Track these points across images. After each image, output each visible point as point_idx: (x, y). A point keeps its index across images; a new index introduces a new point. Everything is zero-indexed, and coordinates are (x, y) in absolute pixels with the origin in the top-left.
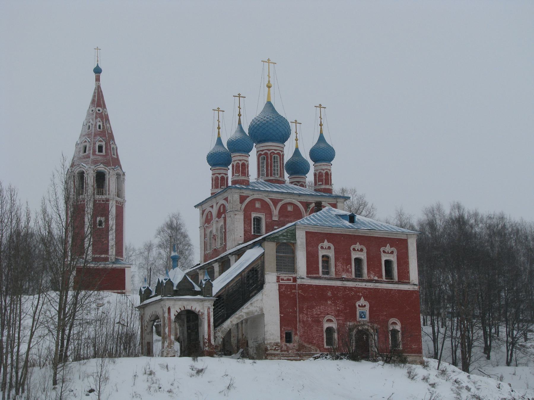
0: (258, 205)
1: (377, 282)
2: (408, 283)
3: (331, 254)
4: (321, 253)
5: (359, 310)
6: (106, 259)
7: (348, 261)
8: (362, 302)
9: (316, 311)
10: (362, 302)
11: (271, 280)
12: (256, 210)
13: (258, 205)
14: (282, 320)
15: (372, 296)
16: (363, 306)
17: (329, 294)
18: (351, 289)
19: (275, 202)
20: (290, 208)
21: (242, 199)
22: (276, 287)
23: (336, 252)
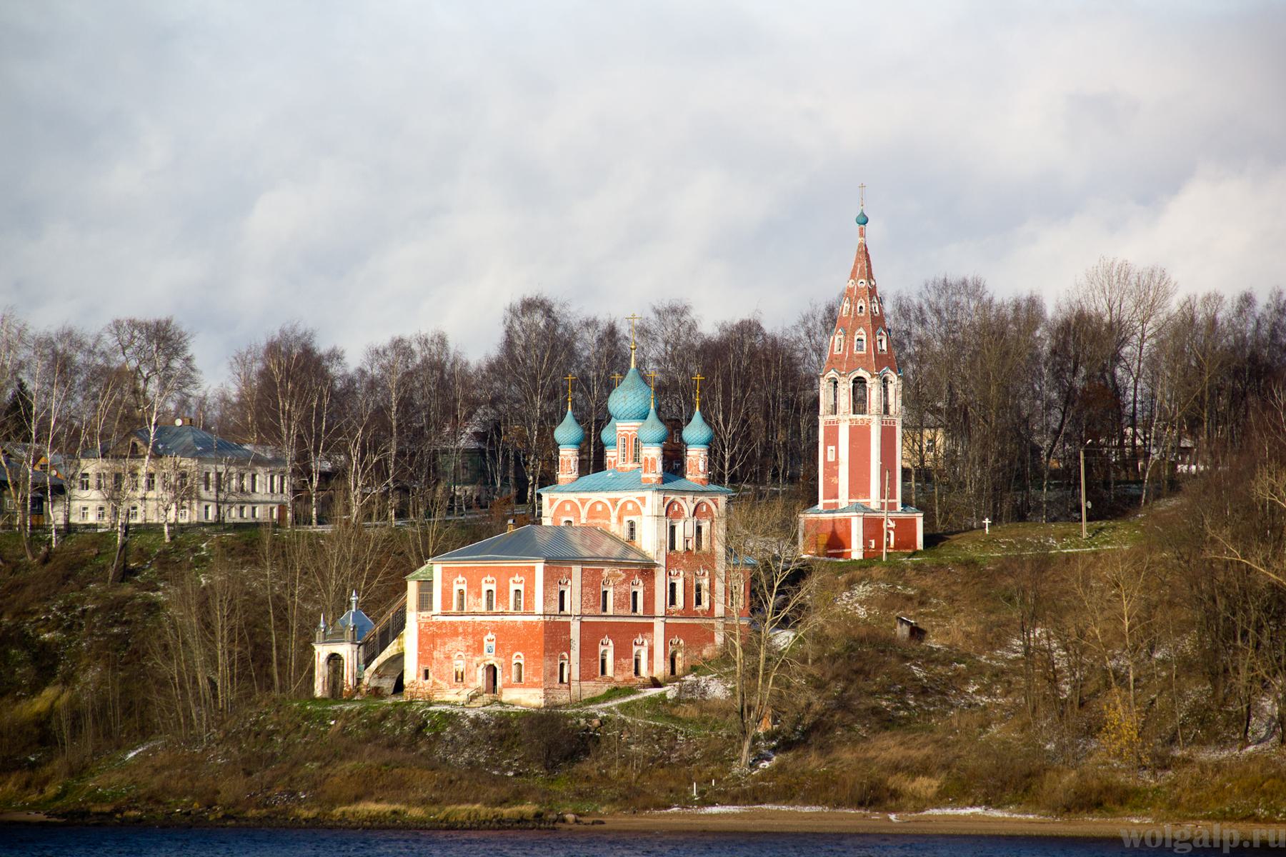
0: (568, 507)
1: (503, 614)
2: (533, 614)
3: (464, 587)
4: (456, 588)
5: (486, 644)
6: (836, 505)
7: (479, 595)
8: (490, 636)
9: (449, 647)
10: (490, 636)
11: (412, 618)
12: (567, 514)
13: (568, 507)
14: (419, 657)
15: (500, 630)
16: (489, 640)
17: (460, 630)
18: (480, 624)
19: (583, 502)
20: (599, 508)
21: (552, 502)
22: (416, 626)
23: (468, 587)
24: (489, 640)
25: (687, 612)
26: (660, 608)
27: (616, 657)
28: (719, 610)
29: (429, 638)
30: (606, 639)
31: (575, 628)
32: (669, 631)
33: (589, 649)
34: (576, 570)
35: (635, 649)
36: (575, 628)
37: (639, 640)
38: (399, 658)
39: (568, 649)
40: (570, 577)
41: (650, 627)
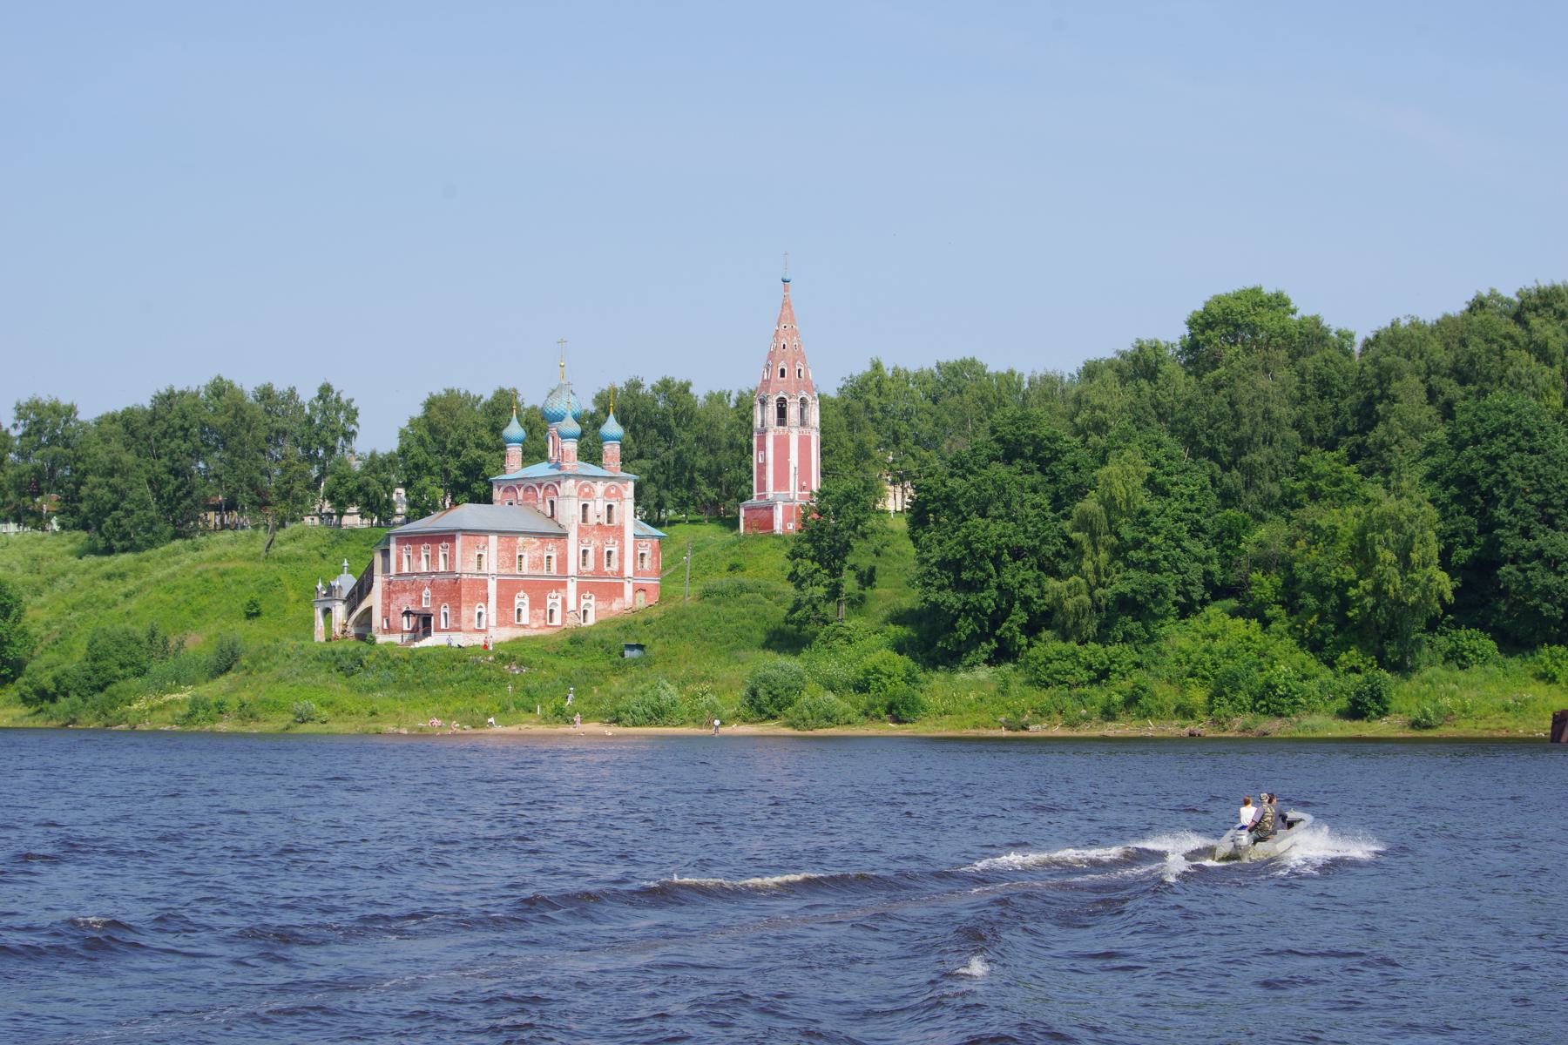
8: (427, 590)
24: (427, 593)
25: (598, 571)
26: (572, 568)
27: (532, 607)
28: (629, 571)
29: (388, 595)
30: (522, 593)
31: (492, 586)
32: (581, 589)
33: (505, 601)
34: (493, 539)
35: (549, 602)
36: (492, 586)
37: (554, 594)
38: (369, 610)
39: (486, 600)
40: (487, 543)
41: (564, 585)
